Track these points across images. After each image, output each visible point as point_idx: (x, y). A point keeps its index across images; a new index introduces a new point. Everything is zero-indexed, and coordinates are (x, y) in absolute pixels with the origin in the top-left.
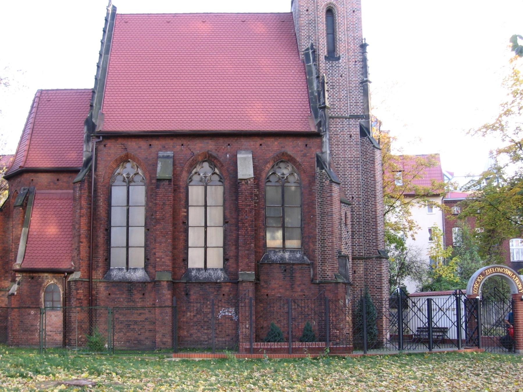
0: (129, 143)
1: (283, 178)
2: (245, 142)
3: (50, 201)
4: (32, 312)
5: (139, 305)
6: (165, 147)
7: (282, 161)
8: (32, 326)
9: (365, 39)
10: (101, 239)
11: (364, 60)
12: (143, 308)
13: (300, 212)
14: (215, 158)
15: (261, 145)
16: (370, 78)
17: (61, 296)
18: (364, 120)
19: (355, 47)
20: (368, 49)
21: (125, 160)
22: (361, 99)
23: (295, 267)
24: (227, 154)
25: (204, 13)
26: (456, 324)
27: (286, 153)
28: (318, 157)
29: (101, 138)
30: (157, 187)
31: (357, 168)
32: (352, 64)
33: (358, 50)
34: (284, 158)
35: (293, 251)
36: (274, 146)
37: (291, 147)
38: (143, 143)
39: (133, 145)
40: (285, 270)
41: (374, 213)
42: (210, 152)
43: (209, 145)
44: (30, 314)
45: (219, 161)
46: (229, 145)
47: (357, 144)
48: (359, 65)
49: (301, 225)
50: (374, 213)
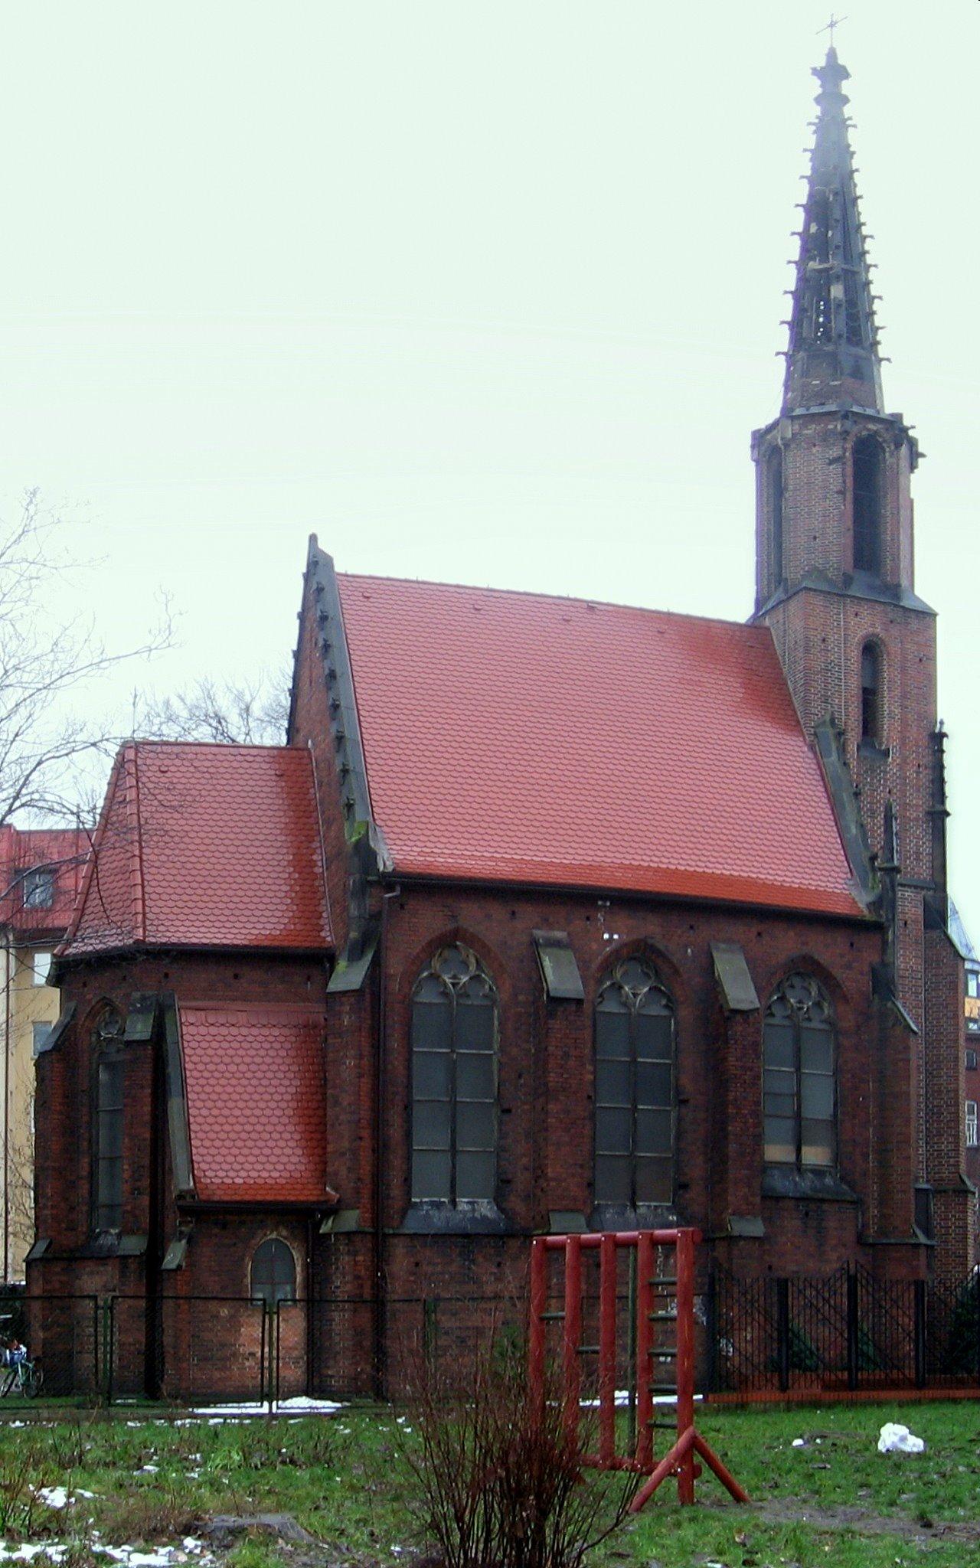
0: (463, 905)
1: (800, 1009)
2: (739, 930)
3: (224, 1031)
4: (224, 1312)
5: (489, 1290)
6: (547, 920)
7: (798, 974)
8: (223, 1345)
9: (942, 723)
10: (395, 1132)
11: (939, 767)
12: (497, 1297)
13: (832, 1086)
14: (660, 954)
15: (759, 934)
16: (949, 806)
17: (298, 1269)
18: (931, 893)
19: (917, 734)
20: (946, 744)
21: (447, 941)
22: (926, 848)
23: (825, 1207)
24: (686, 947)
25: (508, 592)
26: (913, 1335)
27: (811, 958)
28: (873, 971)
29: (398, 888)
30: (551, 1015)
31: (917, 994)
32: (911, 772)
33: (924, 741)
34: (807, 968)
35: (818, 1172)
36: (786, 944)
37: (827, 949)
38: (498, 911)
39: (471, 915)
40: (807, 1214)
41: (952, 1095)
42: (650, 941)
43: (651, 927)
44: (216, 1317)
45: (670, 962)
46: (692, 927)
47: (917, 943)
48: (926, 776)
49: (835, 1115)
50: (952, 1095)
